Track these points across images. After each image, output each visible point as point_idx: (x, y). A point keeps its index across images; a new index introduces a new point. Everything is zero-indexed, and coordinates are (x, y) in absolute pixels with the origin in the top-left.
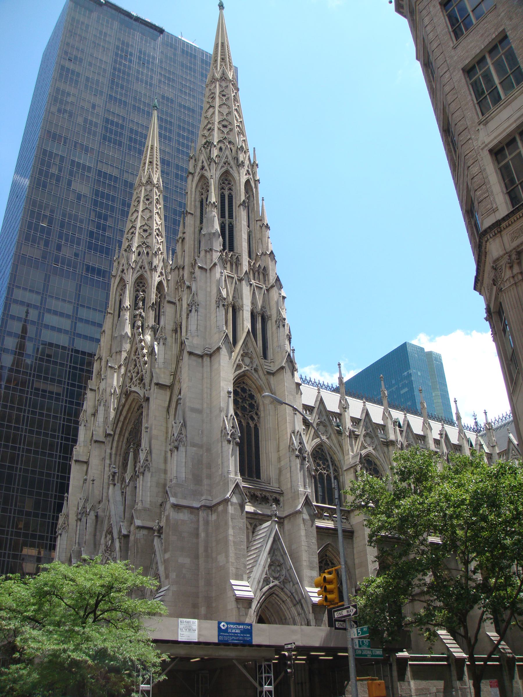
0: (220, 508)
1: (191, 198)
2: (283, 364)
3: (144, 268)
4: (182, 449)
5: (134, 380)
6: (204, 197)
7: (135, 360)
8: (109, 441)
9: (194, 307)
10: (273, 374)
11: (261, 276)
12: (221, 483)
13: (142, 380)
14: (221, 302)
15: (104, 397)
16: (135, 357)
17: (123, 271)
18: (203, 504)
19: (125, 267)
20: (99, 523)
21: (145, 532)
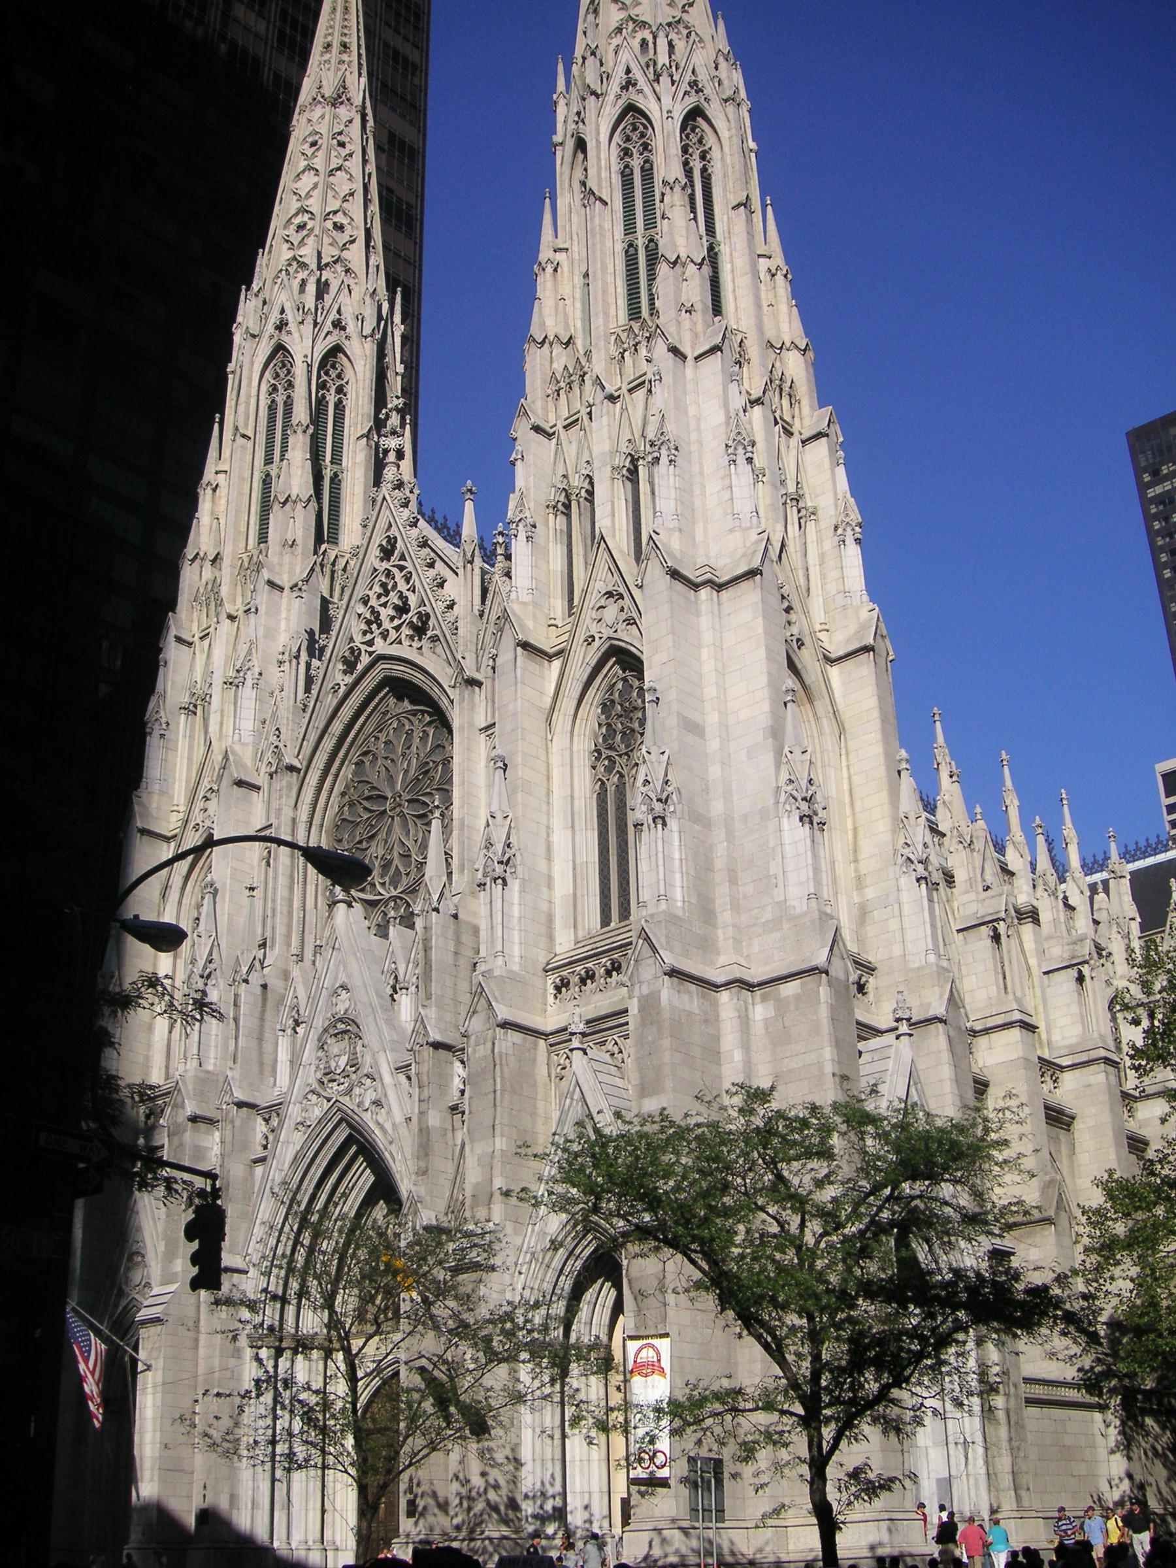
0: (790, 989)
1: (599, 158)
2: (872, 642)
3: (344, 328)
4: (673, 823)
5: (386, 624)
6: (636, 163)
7: (388, 573)
8: (290, 787)
9: (664, 452)
10: (831, 661)
11: (785, 402)
12: (786, 926)
13: (420, 630)
14: (740, 451)
15: (255, 662)
16: (385, 565)
17: (281, 326)
18: (738, 975)
19: (290, 316)
20: (270, 1005)
21: (515, 1037)
